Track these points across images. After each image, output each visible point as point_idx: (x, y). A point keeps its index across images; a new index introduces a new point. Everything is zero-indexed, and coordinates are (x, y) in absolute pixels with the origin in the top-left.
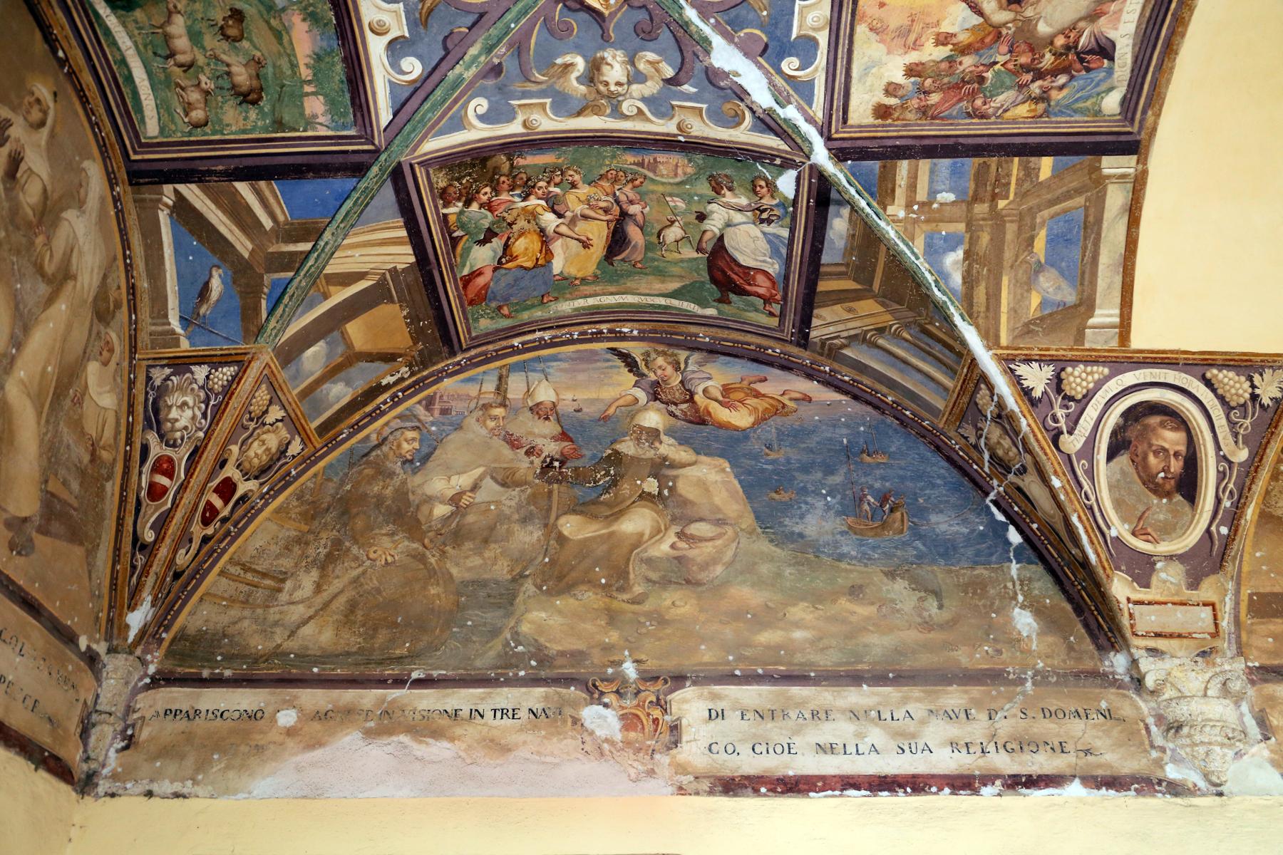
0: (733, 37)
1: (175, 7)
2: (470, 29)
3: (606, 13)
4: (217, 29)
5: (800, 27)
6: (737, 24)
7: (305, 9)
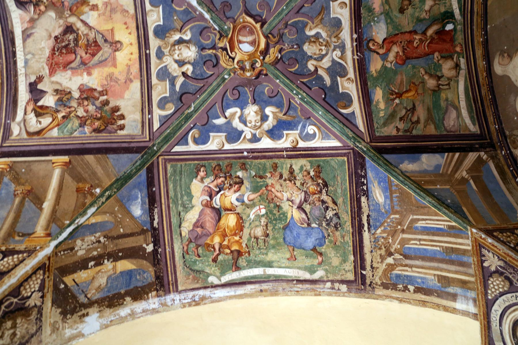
0: (188, 5)
1: (426, 14)
2: (303, 6)
3: (244, 15)
4: (412, 4)
5: (159, 12)
6: (186, 12)
7: (372, 14)
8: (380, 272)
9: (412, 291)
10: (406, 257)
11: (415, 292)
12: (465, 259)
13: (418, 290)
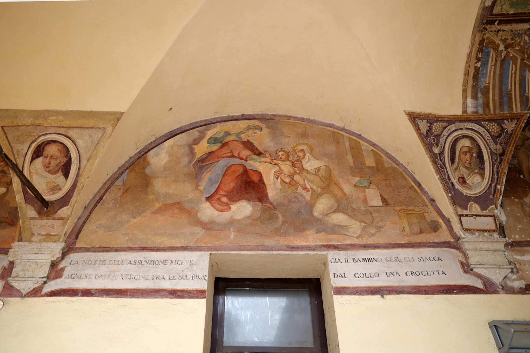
8: (494, 38)
9: (476, 65)
10: (503, 61)
11: (476, 67)
12: (506, 107)
13: (477, 69)
